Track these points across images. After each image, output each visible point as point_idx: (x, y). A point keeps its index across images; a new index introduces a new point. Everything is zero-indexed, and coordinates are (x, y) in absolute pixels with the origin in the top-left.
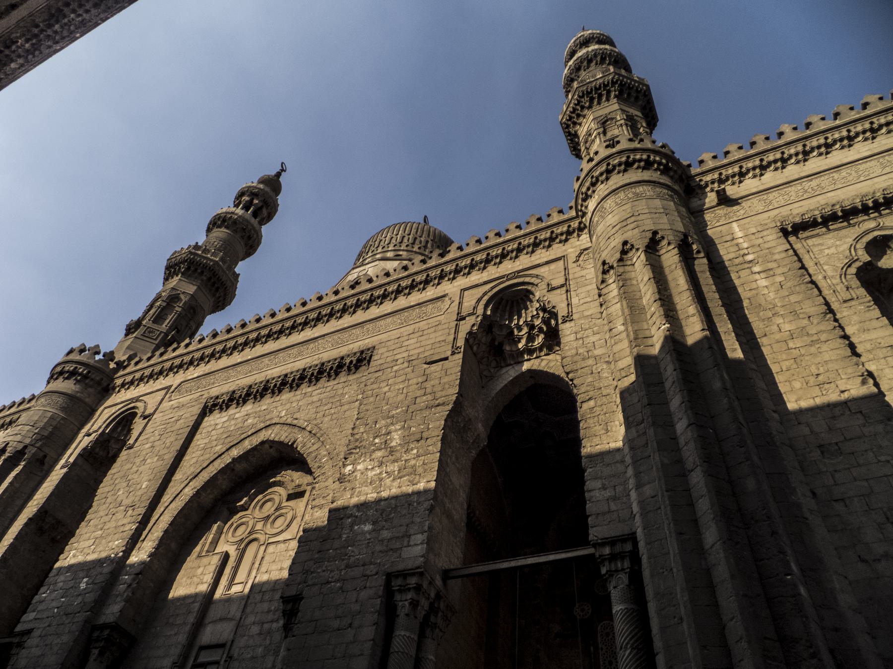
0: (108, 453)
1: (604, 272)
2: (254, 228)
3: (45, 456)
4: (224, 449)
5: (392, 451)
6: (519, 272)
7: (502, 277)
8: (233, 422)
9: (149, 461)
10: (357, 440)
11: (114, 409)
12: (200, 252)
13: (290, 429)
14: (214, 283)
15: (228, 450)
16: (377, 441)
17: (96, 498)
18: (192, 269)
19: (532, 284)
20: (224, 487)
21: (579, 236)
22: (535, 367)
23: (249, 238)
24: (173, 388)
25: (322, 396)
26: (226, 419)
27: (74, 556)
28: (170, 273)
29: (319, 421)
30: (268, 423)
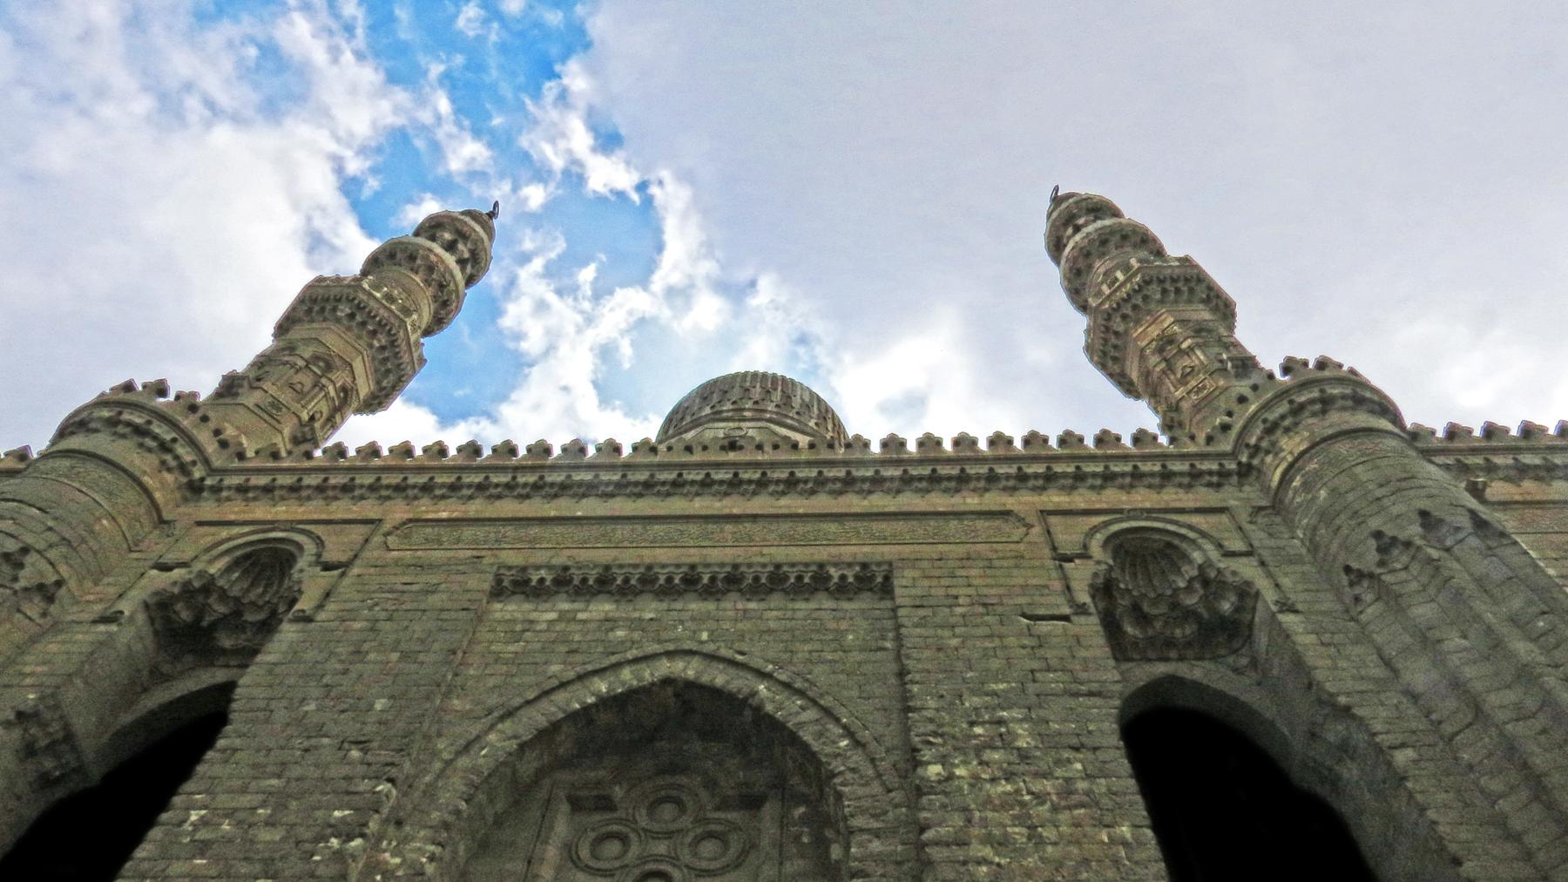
0: (199, 618)
1: (1380, 550)
2: (457, 291)
3: (59, 584)
4: (571, 675)
5: (1024, 756)
6: (1149, 511)
7: (1120, 511)
8: (573, 627)
9: (372, 656)
10: (931, 720)
11: (224, 533)
12: (378, 295)
13: (732, 671)
14: (386, 360)
15: (580, 678)
16: (978, 730)
17: (234, 706)
18: (359, 318)
19: (1183, 537)
20: (561, 751)
21: (1240, 485)
22: (1180, 674)
23: (445, 304)
24: (387, 527)
25: (789, 624)
26: (553, 616)
27: (203, 822)
28: (309, 311)
29: (800, 668)
30: (671, 647)
